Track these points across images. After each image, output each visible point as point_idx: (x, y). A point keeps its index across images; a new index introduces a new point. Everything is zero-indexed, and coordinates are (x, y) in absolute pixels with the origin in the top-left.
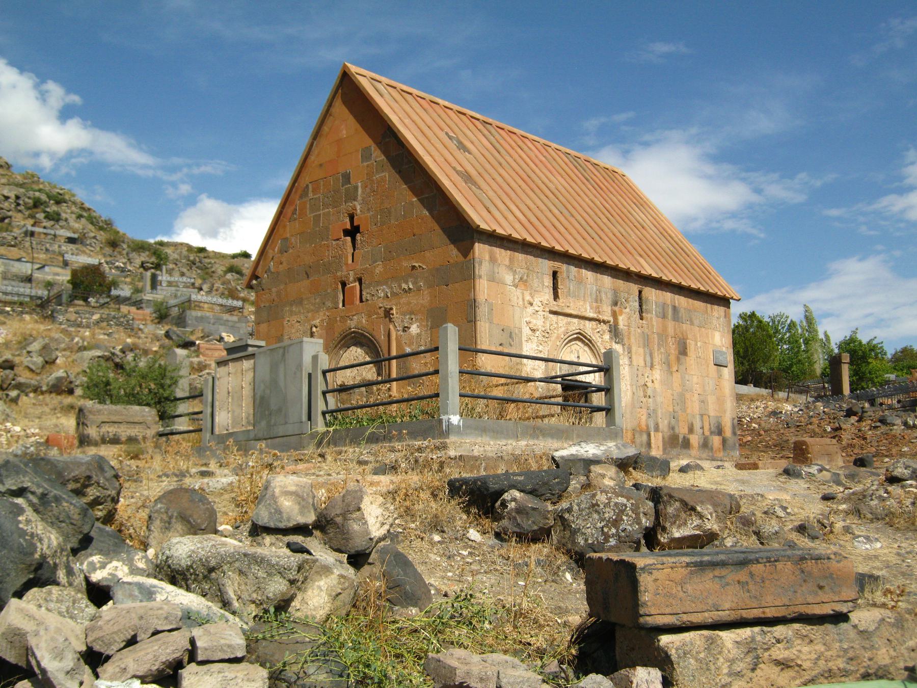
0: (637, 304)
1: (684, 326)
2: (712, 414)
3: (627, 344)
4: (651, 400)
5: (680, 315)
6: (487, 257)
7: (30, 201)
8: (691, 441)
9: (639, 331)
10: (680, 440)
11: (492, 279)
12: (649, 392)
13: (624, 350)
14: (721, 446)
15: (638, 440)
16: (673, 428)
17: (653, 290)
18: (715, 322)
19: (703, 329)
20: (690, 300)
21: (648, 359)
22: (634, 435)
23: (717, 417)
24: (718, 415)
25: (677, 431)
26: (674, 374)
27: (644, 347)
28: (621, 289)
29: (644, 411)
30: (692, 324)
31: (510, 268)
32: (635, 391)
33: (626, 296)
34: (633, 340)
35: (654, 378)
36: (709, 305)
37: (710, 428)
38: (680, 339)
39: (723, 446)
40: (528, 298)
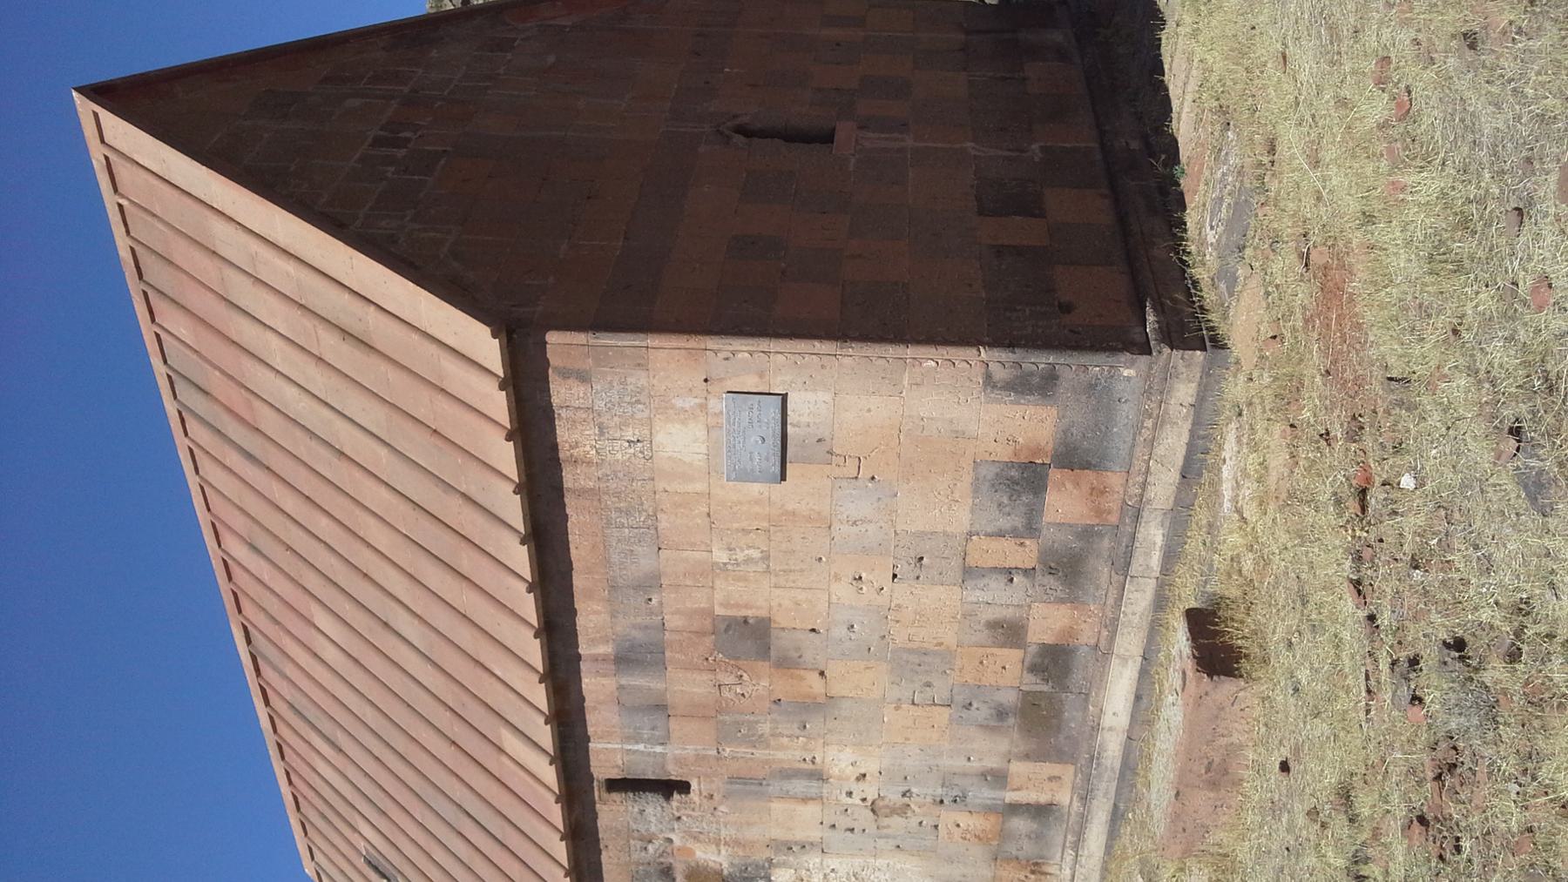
1: (673, 621)
2: (960, 518)
3: (768, 853)
4: (914, 790)
5: (638, 635)
8: (1049, 639)
9: (722, 808)
10: (1045, 688)
12: (894, 797)
13: (784, 865)
14: (1089, 476)
15: (1028, 849)
16: (1001, 713)
17: (591, 745)
18: (620, 453)
19: (664, 522)
20: (579, 581)
21: (799, 786)
22: (1008, 860)
23: (976, 490)
24: (968, 479)
25: (1009, 698)
26: (837, 689)
28: (624, 858)
29: (948, 817)
30: (649, 584)
32: (892, 843)
33: (639, 844)
34: (752, 834)
35: (852, 772)
36: (569, 478)
37: (1015, 533)
39: (1087, 466)
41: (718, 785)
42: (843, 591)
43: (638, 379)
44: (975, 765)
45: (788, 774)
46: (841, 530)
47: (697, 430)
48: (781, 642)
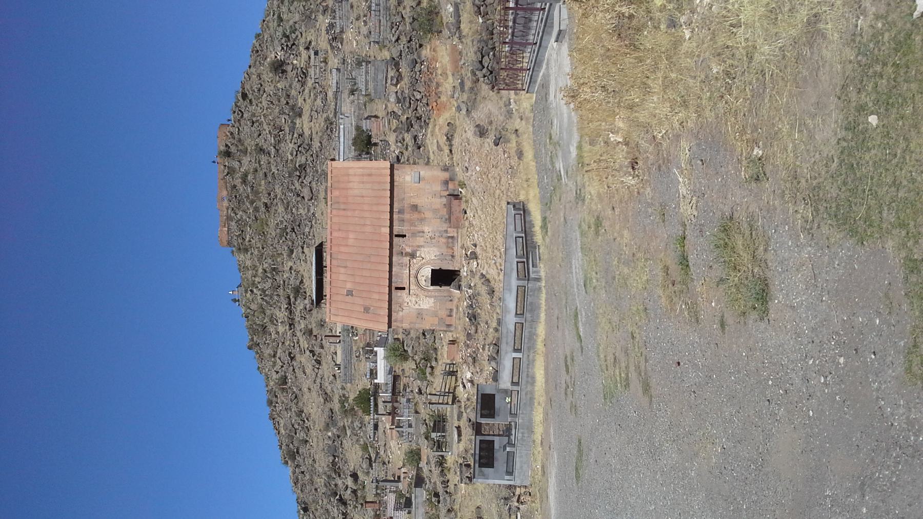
0: (401, 239)
1: (406, 206)
6: (395, 323)
7: (284, 39)
11: (402, 322)
12: (433, 236)
15: (450, 245)
21: (421, 234)
27: (416, 237)
30: (404, 199)
31: (397, 312)
34: (414, 244)
36: (395, 184)
37: (446, 190)
38: (411, 210)
40: (406, 304)
41: (410, 235)
42: (426, 200)
43: (404, 170)
44: (443, 229)
45: (419, 232)
46: (426, 190)
47: (410, 177)
48: (419, 208)
